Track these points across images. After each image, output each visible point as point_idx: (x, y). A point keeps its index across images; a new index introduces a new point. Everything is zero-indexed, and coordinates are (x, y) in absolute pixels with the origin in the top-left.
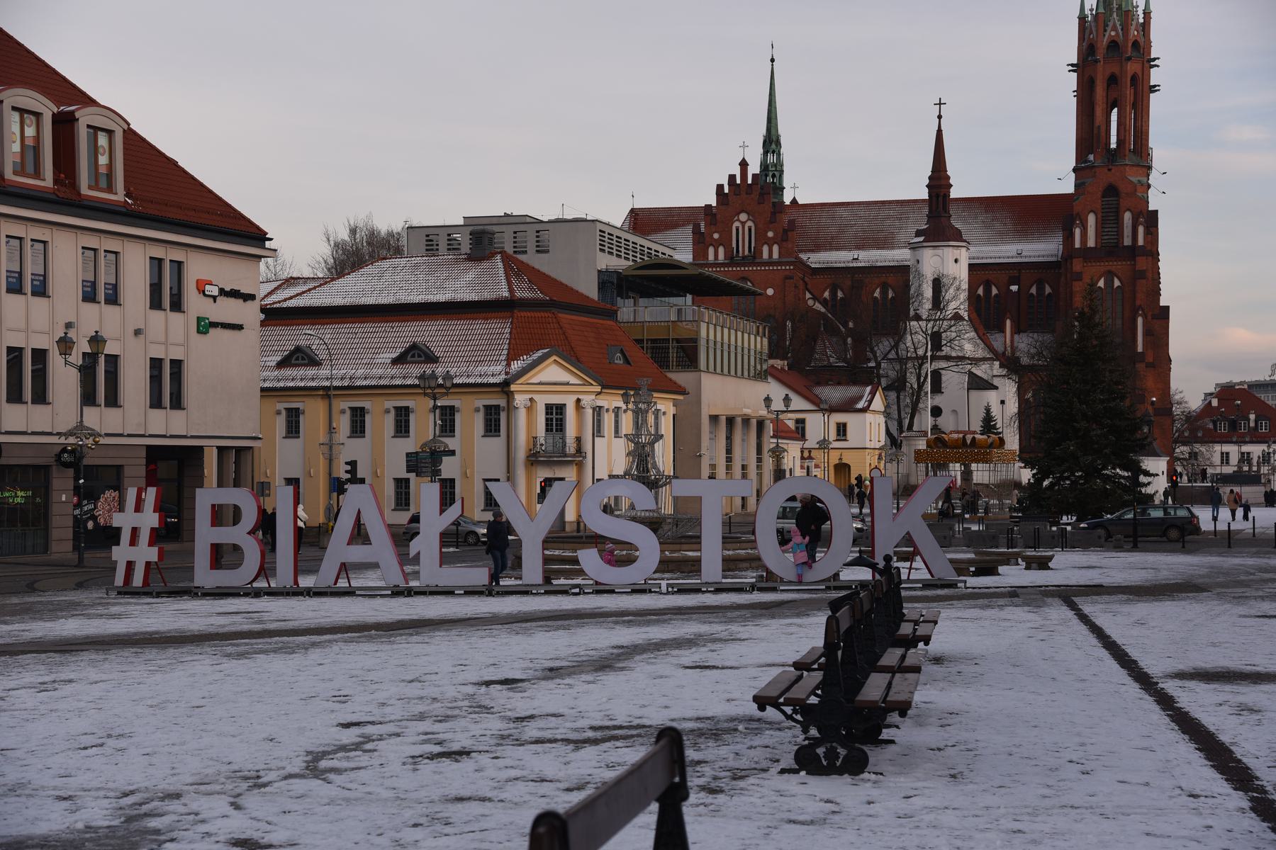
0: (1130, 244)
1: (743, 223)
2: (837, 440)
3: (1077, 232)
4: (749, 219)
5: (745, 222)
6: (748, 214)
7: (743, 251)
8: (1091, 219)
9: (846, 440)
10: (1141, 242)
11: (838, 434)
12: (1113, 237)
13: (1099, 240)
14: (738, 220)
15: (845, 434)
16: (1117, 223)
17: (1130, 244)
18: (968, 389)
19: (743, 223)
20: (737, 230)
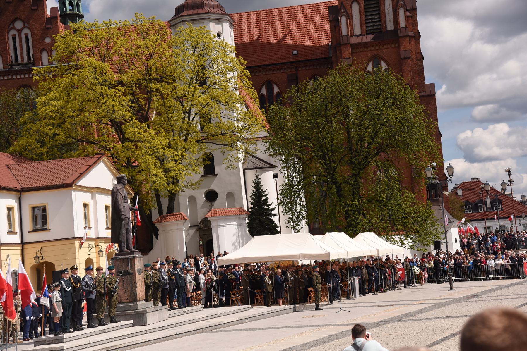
0: (393, 28)
1: (20, 31)
2: (34, 231)
3: (343, 20)
4: (24, 27)
5: (22, 29)
6: (23, 22)
7: (22, 58)
8: (355, 9)
9: (46, 229)
10: (402, 23)
11: (35, 223)
12: (376, 24)
13: (364, 27)
14: (14, 28)
15: (45, 223)
16: (379, 10)
17: (393, 28)
18: (244, 170)
19: (20, 31)
20: (14, 38)
